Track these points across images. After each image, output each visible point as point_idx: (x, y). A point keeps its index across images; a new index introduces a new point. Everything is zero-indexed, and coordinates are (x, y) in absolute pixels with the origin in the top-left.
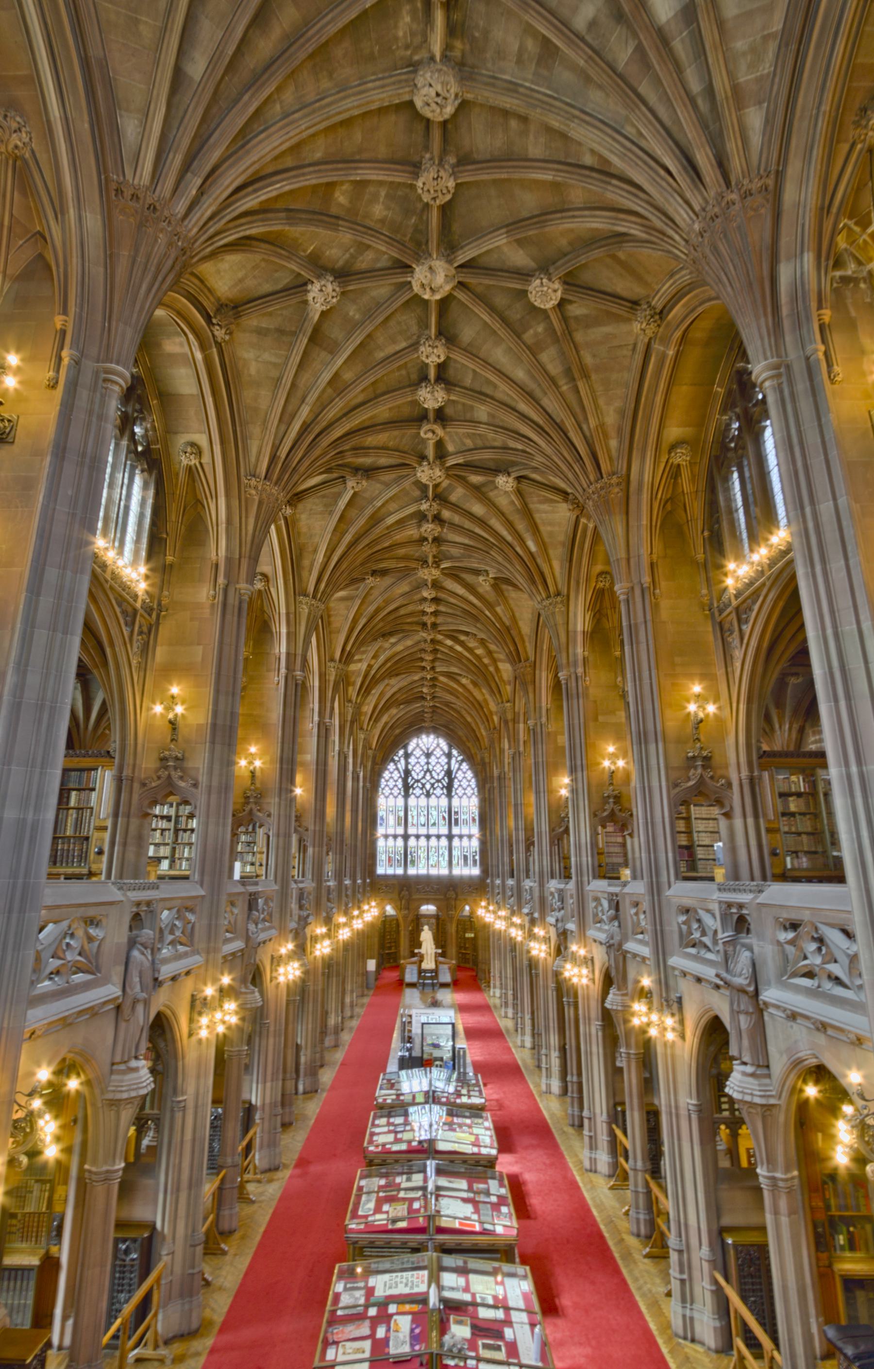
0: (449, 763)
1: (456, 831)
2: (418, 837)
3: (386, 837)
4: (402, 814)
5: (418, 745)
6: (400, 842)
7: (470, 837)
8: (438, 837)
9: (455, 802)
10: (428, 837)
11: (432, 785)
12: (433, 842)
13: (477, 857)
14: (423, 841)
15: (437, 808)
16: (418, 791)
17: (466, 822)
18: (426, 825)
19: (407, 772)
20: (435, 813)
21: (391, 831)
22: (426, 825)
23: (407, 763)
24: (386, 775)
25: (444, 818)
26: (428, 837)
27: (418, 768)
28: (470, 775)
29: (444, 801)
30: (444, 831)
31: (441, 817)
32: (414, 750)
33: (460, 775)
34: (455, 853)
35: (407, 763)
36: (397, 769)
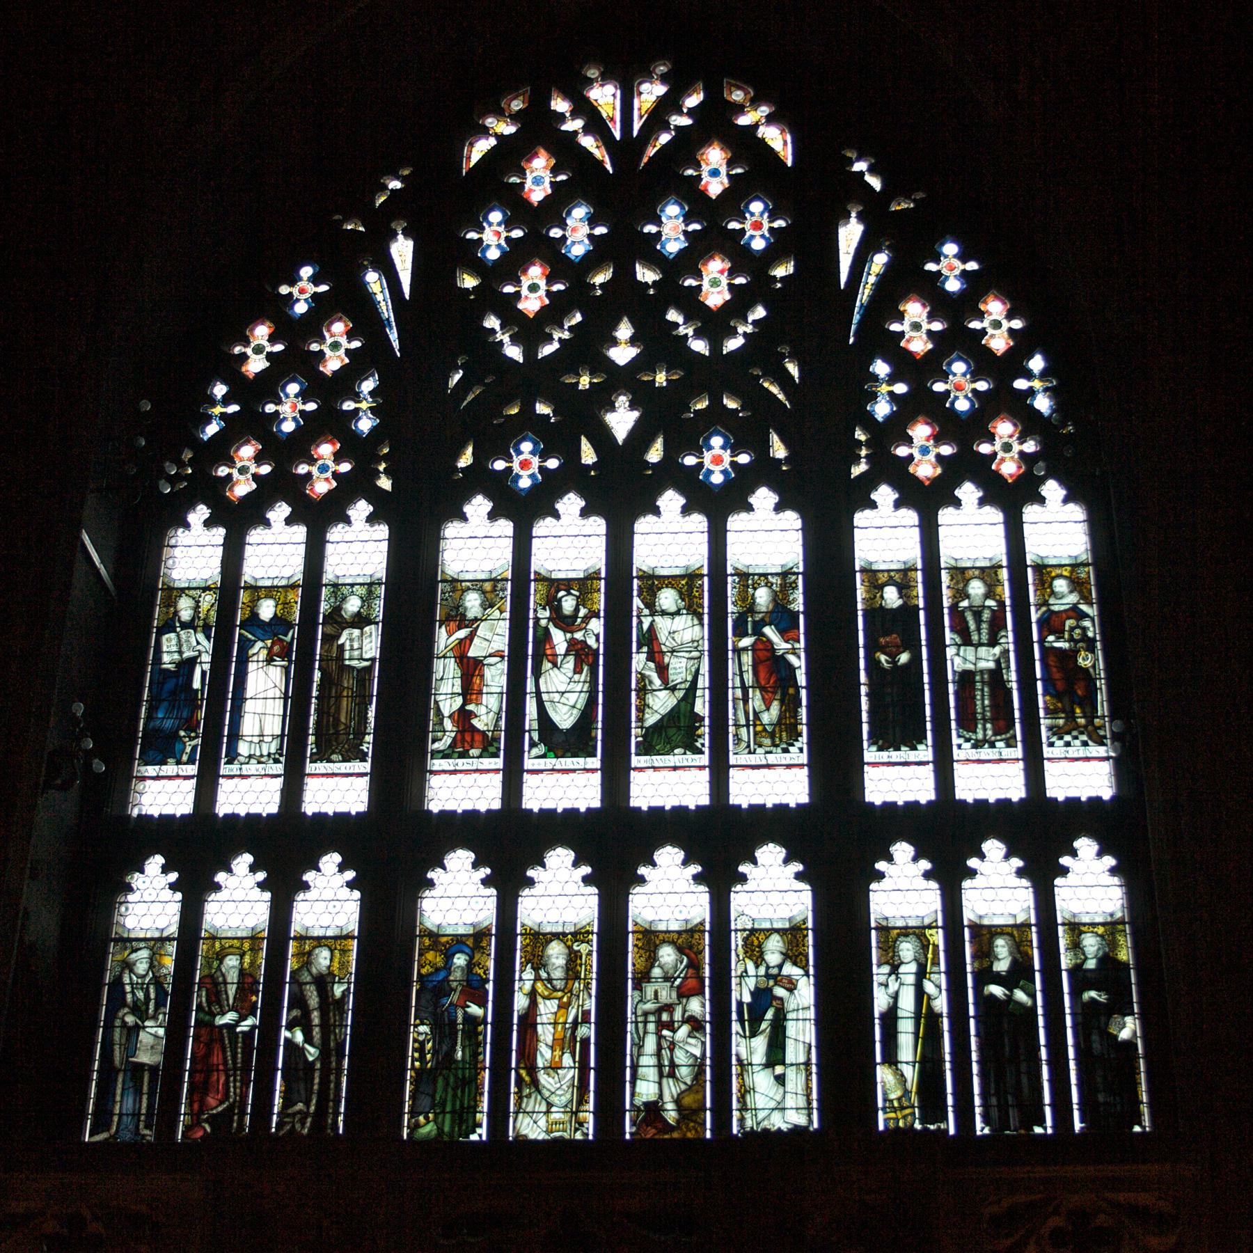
0: (808, 240)
2: (510, 844)
3: (198, 849)
4: (365, 646)
5: (539, 130)
6: (330, 902)
7: (1039, 832)
8: (717, 843)
9: (883, 536)
10: (614, 844)
11: (660, 415)
12: (668, 892)
13: (1128, 1029)
14: (560, 894)
15: (711, 588)
16: (526, 464)
17: (994, 710)
18: (608, 733)
19: (442, 316)
20: (682, 632)
21: (249, 793)
22: (608, 733)
23: (443, 252)
24: (258, 350)
25: (773, 672)
26: (614, 844)
27: (533, 290)
28: (997, 324)
29: (768, 538)
30: (776, 780)
31: (741, 669)
32: (510, 155)
33: (916, 325)
34: (891, 991)
35: (443, 252)
36: (347, 300)
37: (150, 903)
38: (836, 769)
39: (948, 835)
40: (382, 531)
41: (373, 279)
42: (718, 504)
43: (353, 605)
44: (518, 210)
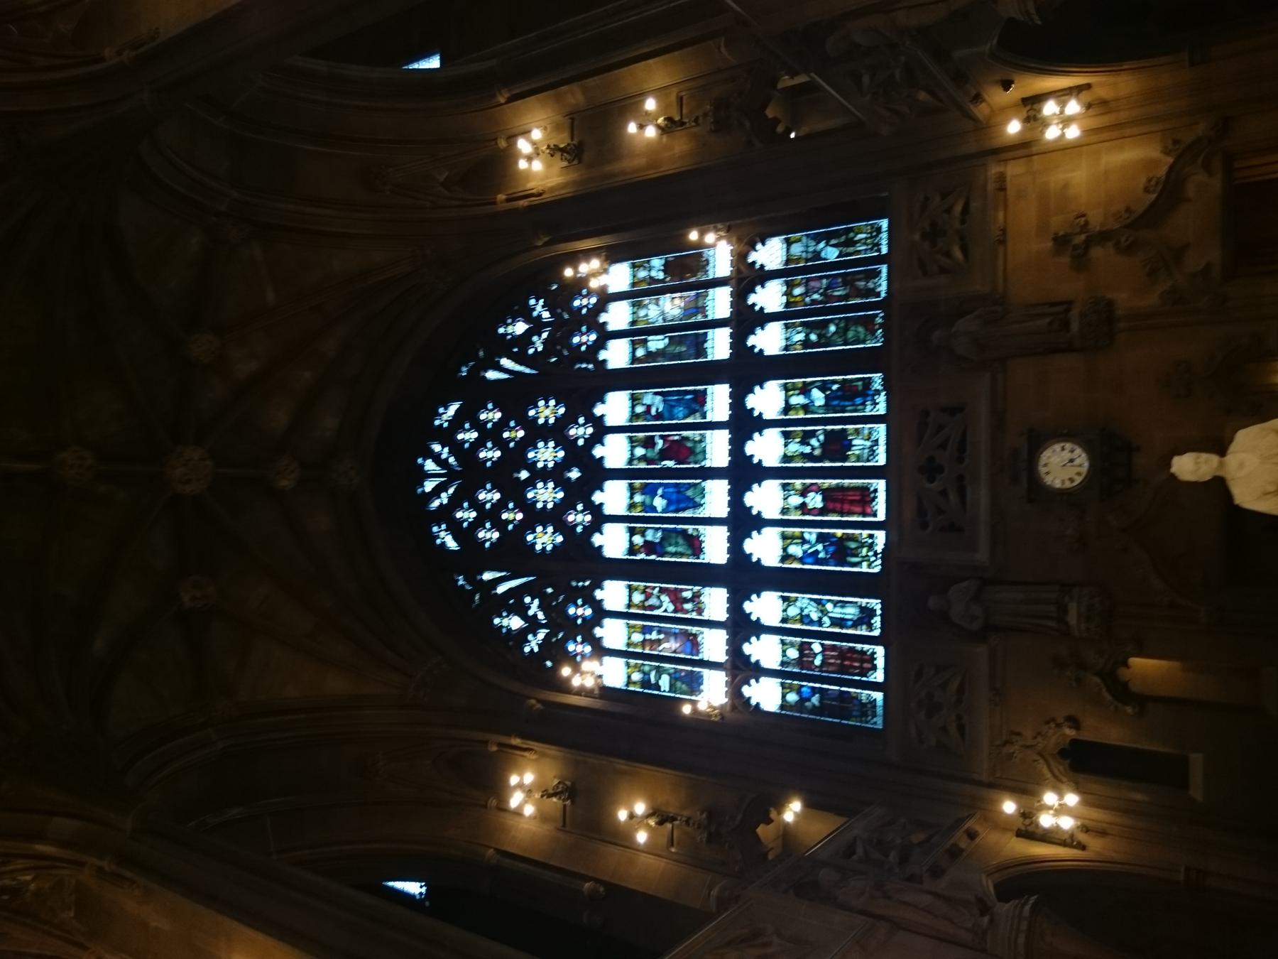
1: (719, 345)
2: (742, 522)
3: (741, 668)
6: (766, 606)
10: (744, 473)
12: (767, 448)
14: (766, 498)
26: (744, 473)
29: (615, 408)
30: (719, 400)
37: (766, 695)
38: (715, 372)
39: (746, 320)
40: (608, 584)
41: (501, 589)
42: (601, 431)
43: (637, 598)
44: (478, 524)
